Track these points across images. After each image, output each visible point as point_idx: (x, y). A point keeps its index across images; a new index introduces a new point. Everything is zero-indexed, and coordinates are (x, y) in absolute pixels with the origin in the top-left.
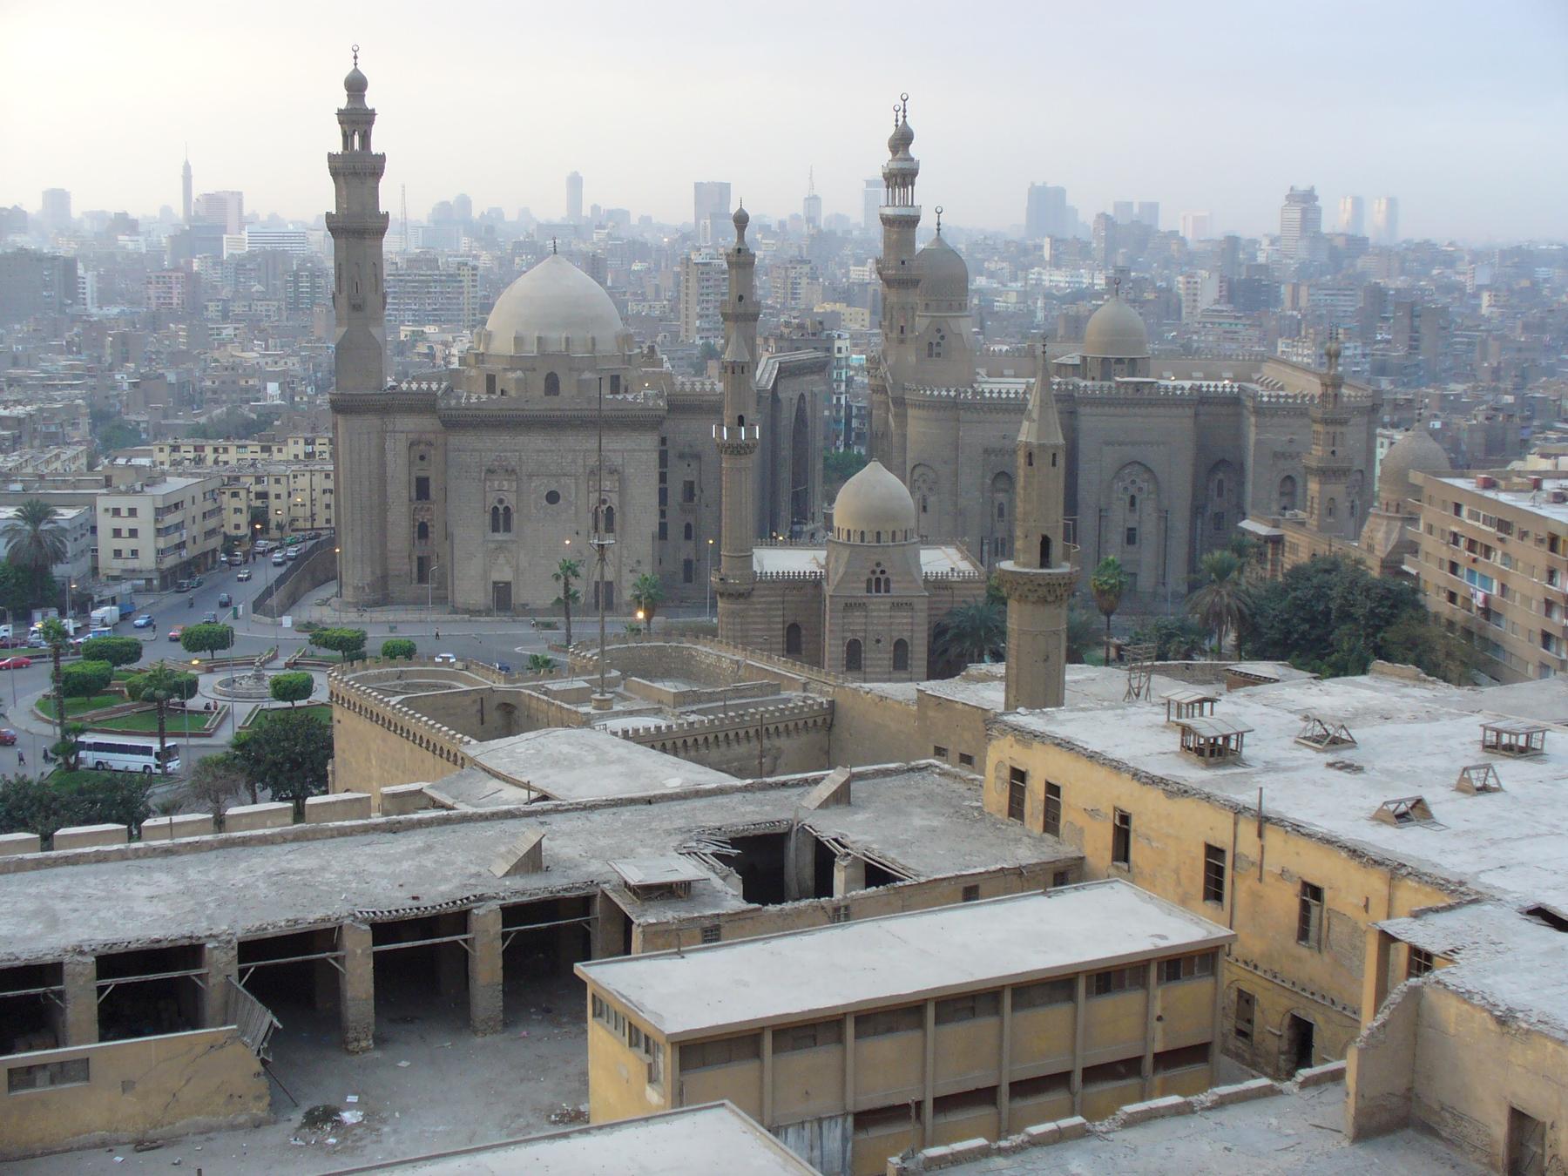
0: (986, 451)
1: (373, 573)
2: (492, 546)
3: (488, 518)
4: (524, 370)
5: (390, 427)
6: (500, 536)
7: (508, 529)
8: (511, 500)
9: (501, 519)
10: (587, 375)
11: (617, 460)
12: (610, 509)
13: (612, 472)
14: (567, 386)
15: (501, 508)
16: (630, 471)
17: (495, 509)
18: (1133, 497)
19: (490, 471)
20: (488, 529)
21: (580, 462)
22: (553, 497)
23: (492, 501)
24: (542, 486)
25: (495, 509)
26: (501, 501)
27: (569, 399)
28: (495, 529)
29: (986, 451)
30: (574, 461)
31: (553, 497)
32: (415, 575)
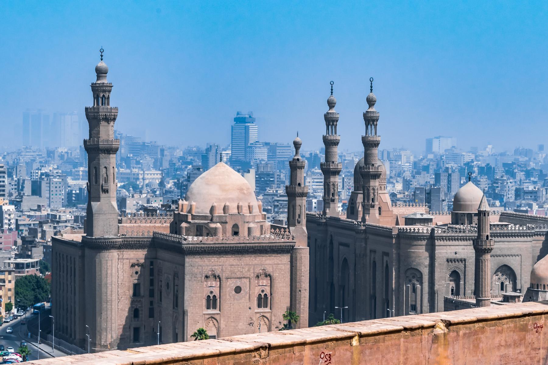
0: (448, 261)
1: (112, 337)
2: (207, 316)
3: (204, 302)
4: (221, 223)
5: (121, 257)
6: (211, 311)
7: (215, 307)
8: (216, 292)
9: (212, 302)
10: (252, 225)
11: (269, 270)
12: (266, 295)
13: (267, 275)
14: (243, 232)
15: (211, 296)
16: (275, 275)
17: (209, 296)
18: (502, 284)
19: (207, 277)
20: (204, 308)
21: (252, 271)
22: (238, 290)
23: (206, 293)
24: (231, 284)
25: (209, 296)
26: (211, 292)
27: (243, 238)
28: (208, 308)
29: (448, 261)
30: (249, 270)
31: (238, 290)
32: (132, 337)
